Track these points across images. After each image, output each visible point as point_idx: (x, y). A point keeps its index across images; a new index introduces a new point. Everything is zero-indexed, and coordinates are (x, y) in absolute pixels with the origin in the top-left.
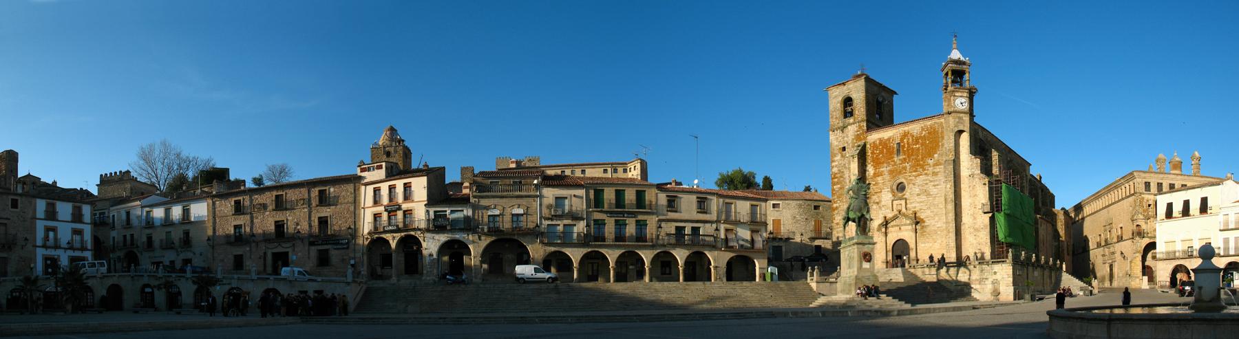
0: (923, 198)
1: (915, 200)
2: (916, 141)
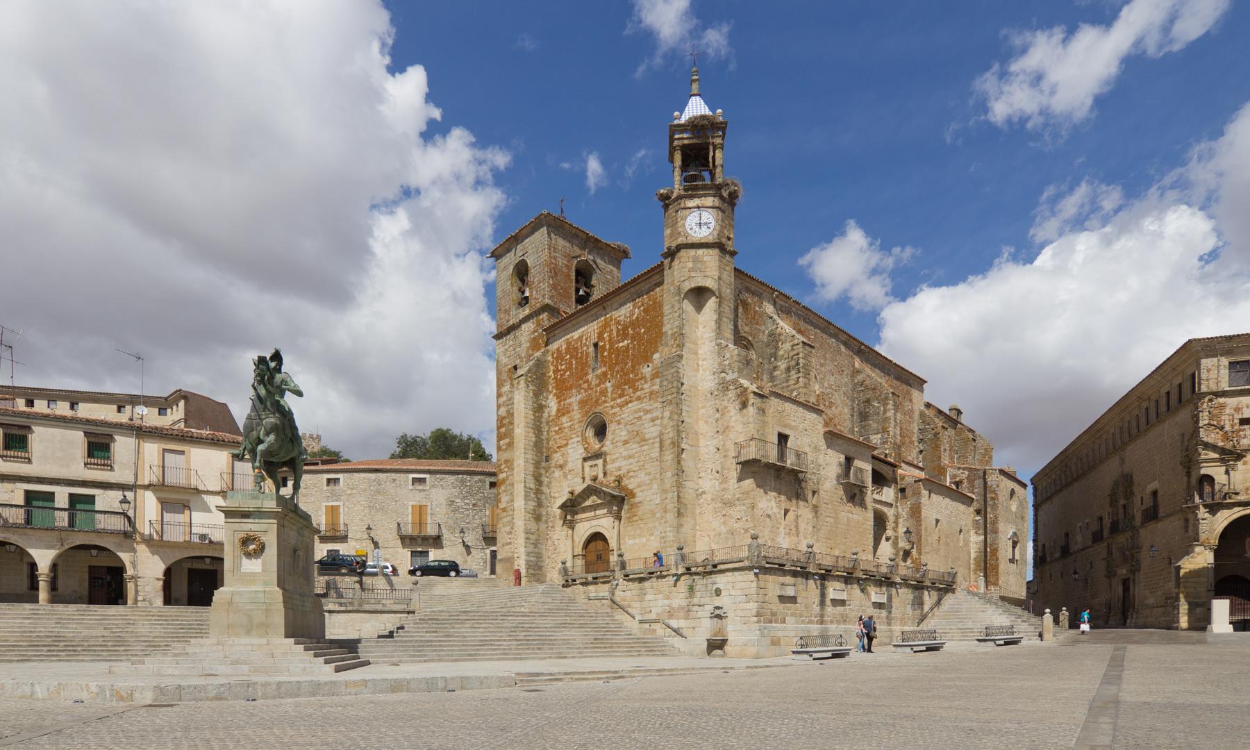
0: (634, 447)
1: (624, 458)
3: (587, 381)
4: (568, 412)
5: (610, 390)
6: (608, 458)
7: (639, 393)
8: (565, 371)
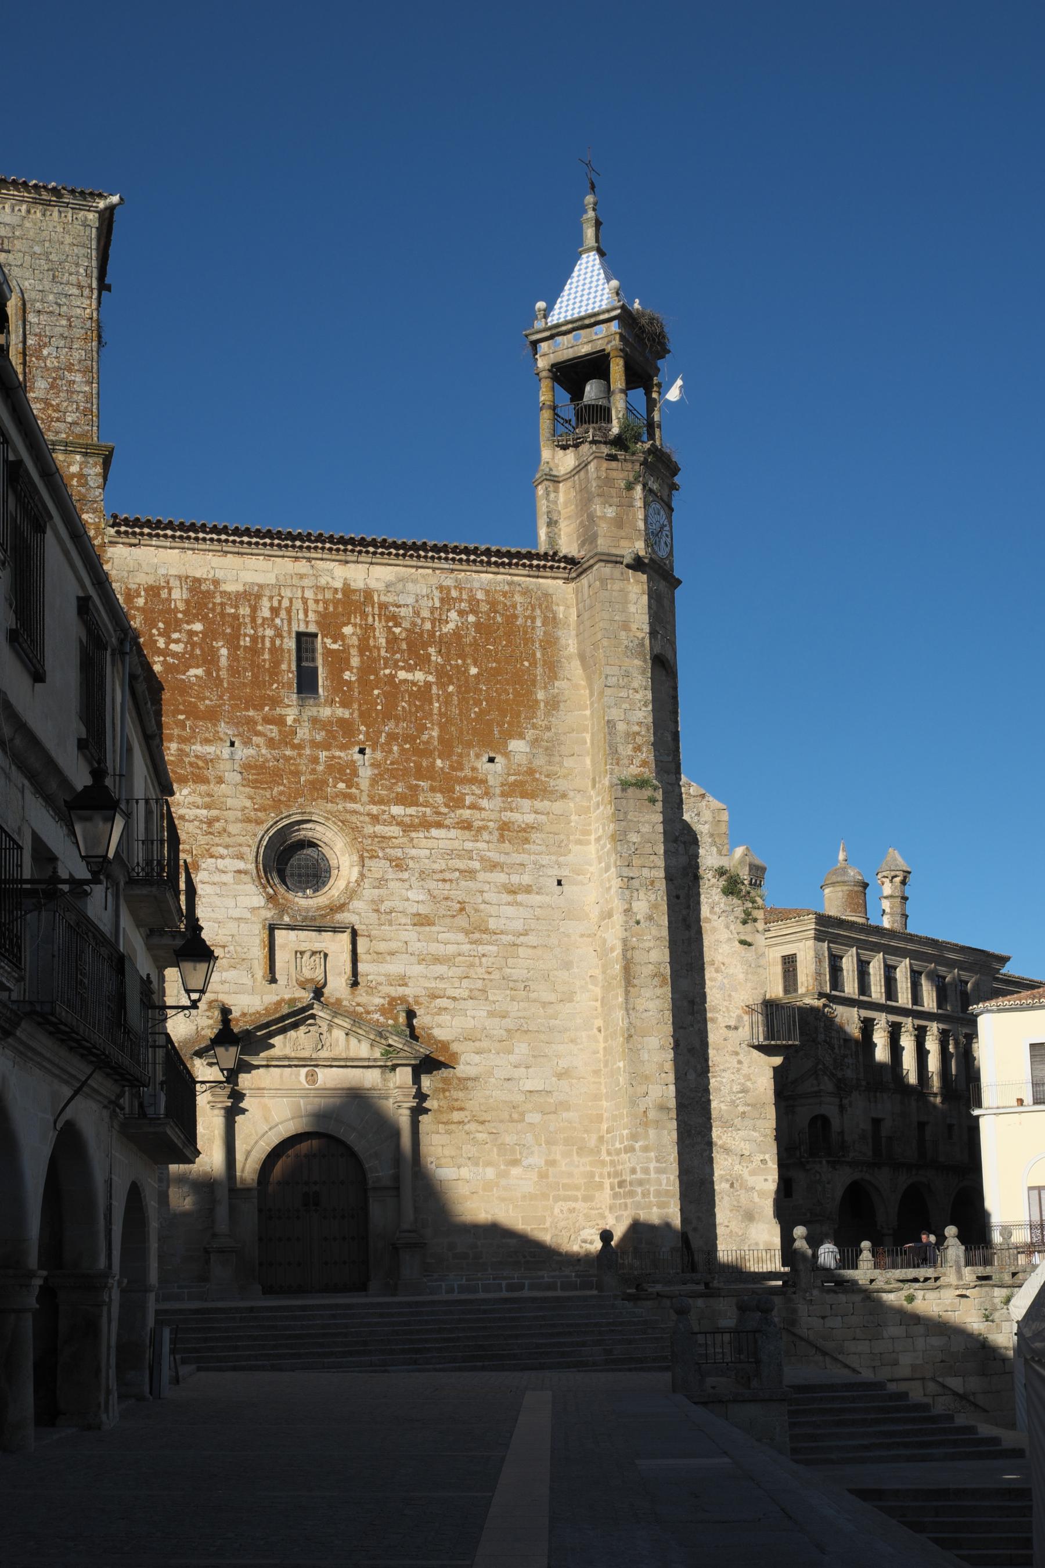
0: (449, 940)
2: (415, 647)
3: (280, 721)
4: (202, 780)
5: (365, 773)
6: (362, 944)
7: (466, 813)
8: (186, 662)
